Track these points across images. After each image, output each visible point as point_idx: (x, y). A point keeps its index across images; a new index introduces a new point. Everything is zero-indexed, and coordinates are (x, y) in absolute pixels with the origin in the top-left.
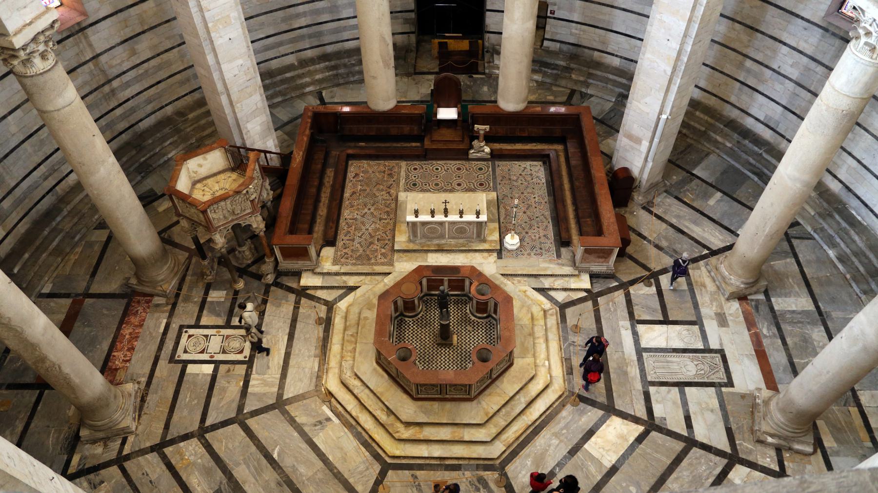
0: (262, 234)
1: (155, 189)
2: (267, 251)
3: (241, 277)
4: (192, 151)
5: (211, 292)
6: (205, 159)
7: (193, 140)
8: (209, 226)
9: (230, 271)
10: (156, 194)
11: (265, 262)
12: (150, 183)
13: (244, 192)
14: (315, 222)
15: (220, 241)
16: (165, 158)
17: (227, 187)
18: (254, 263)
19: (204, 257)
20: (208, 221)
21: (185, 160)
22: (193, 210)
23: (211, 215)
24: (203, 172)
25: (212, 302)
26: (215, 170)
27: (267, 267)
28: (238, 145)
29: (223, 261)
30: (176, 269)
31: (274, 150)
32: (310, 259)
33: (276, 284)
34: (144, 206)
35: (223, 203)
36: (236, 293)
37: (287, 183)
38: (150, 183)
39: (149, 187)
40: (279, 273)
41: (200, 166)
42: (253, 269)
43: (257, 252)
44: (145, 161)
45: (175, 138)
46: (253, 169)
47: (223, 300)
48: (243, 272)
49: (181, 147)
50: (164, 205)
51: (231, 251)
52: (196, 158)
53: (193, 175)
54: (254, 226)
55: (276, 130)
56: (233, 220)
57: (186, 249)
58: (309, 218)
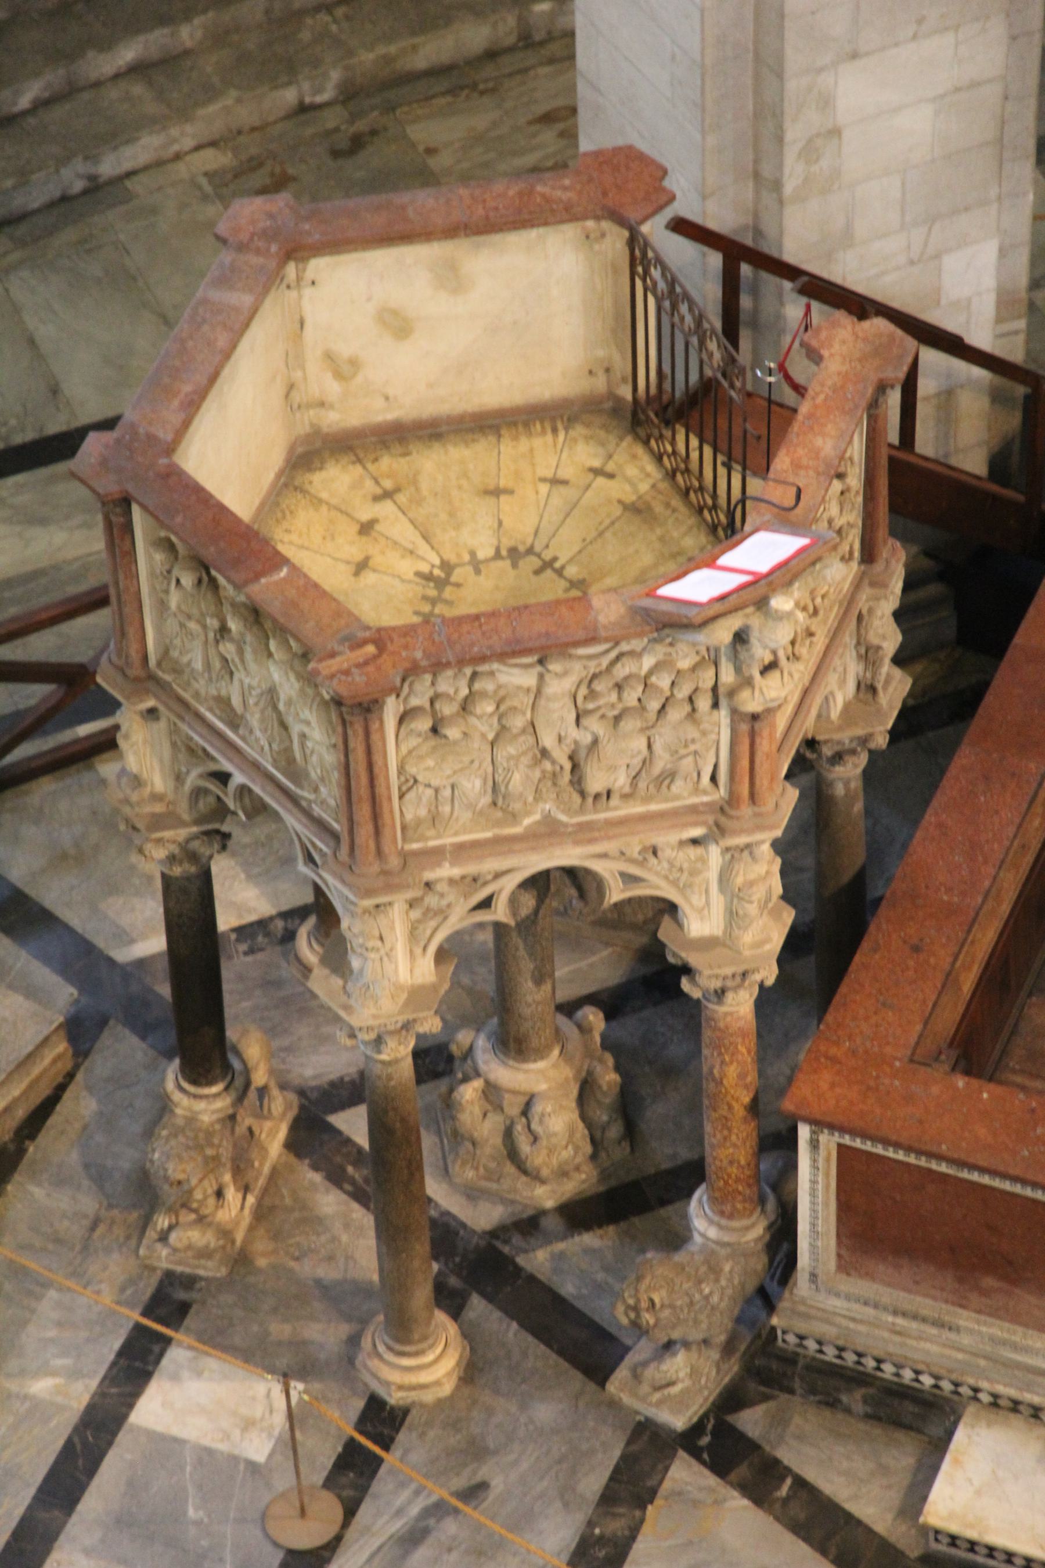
0: (740, 1007)
2: (731, 1146)
3: (449, 1300)
6: (452, 280)
9: (391, 1235)
13: (722, 633)
15: (393, 973)
17: (563, 550)
18: (579, 1215)
20: (363, 786)
21: (297, 251)
23: (396, 745)
24: (406, 380)
25: (165, 1447)
26: (498, 388)
29: (371, 1138)
31: (981, 338)
33: (722, 1445)
35: (516, 677)
36: (382, 1419)
40: (766, 1364)
41: (398, 325)
42: (560, 1262)
43: (631, 1131)
45: (188, 34)
47: (258, 1449)
48: (479, 1271)
49: (214, 116)
52: (381, 258)
53: (321, 383)
54: (701, 921)
56: (549, 832)
57: (83, 960)
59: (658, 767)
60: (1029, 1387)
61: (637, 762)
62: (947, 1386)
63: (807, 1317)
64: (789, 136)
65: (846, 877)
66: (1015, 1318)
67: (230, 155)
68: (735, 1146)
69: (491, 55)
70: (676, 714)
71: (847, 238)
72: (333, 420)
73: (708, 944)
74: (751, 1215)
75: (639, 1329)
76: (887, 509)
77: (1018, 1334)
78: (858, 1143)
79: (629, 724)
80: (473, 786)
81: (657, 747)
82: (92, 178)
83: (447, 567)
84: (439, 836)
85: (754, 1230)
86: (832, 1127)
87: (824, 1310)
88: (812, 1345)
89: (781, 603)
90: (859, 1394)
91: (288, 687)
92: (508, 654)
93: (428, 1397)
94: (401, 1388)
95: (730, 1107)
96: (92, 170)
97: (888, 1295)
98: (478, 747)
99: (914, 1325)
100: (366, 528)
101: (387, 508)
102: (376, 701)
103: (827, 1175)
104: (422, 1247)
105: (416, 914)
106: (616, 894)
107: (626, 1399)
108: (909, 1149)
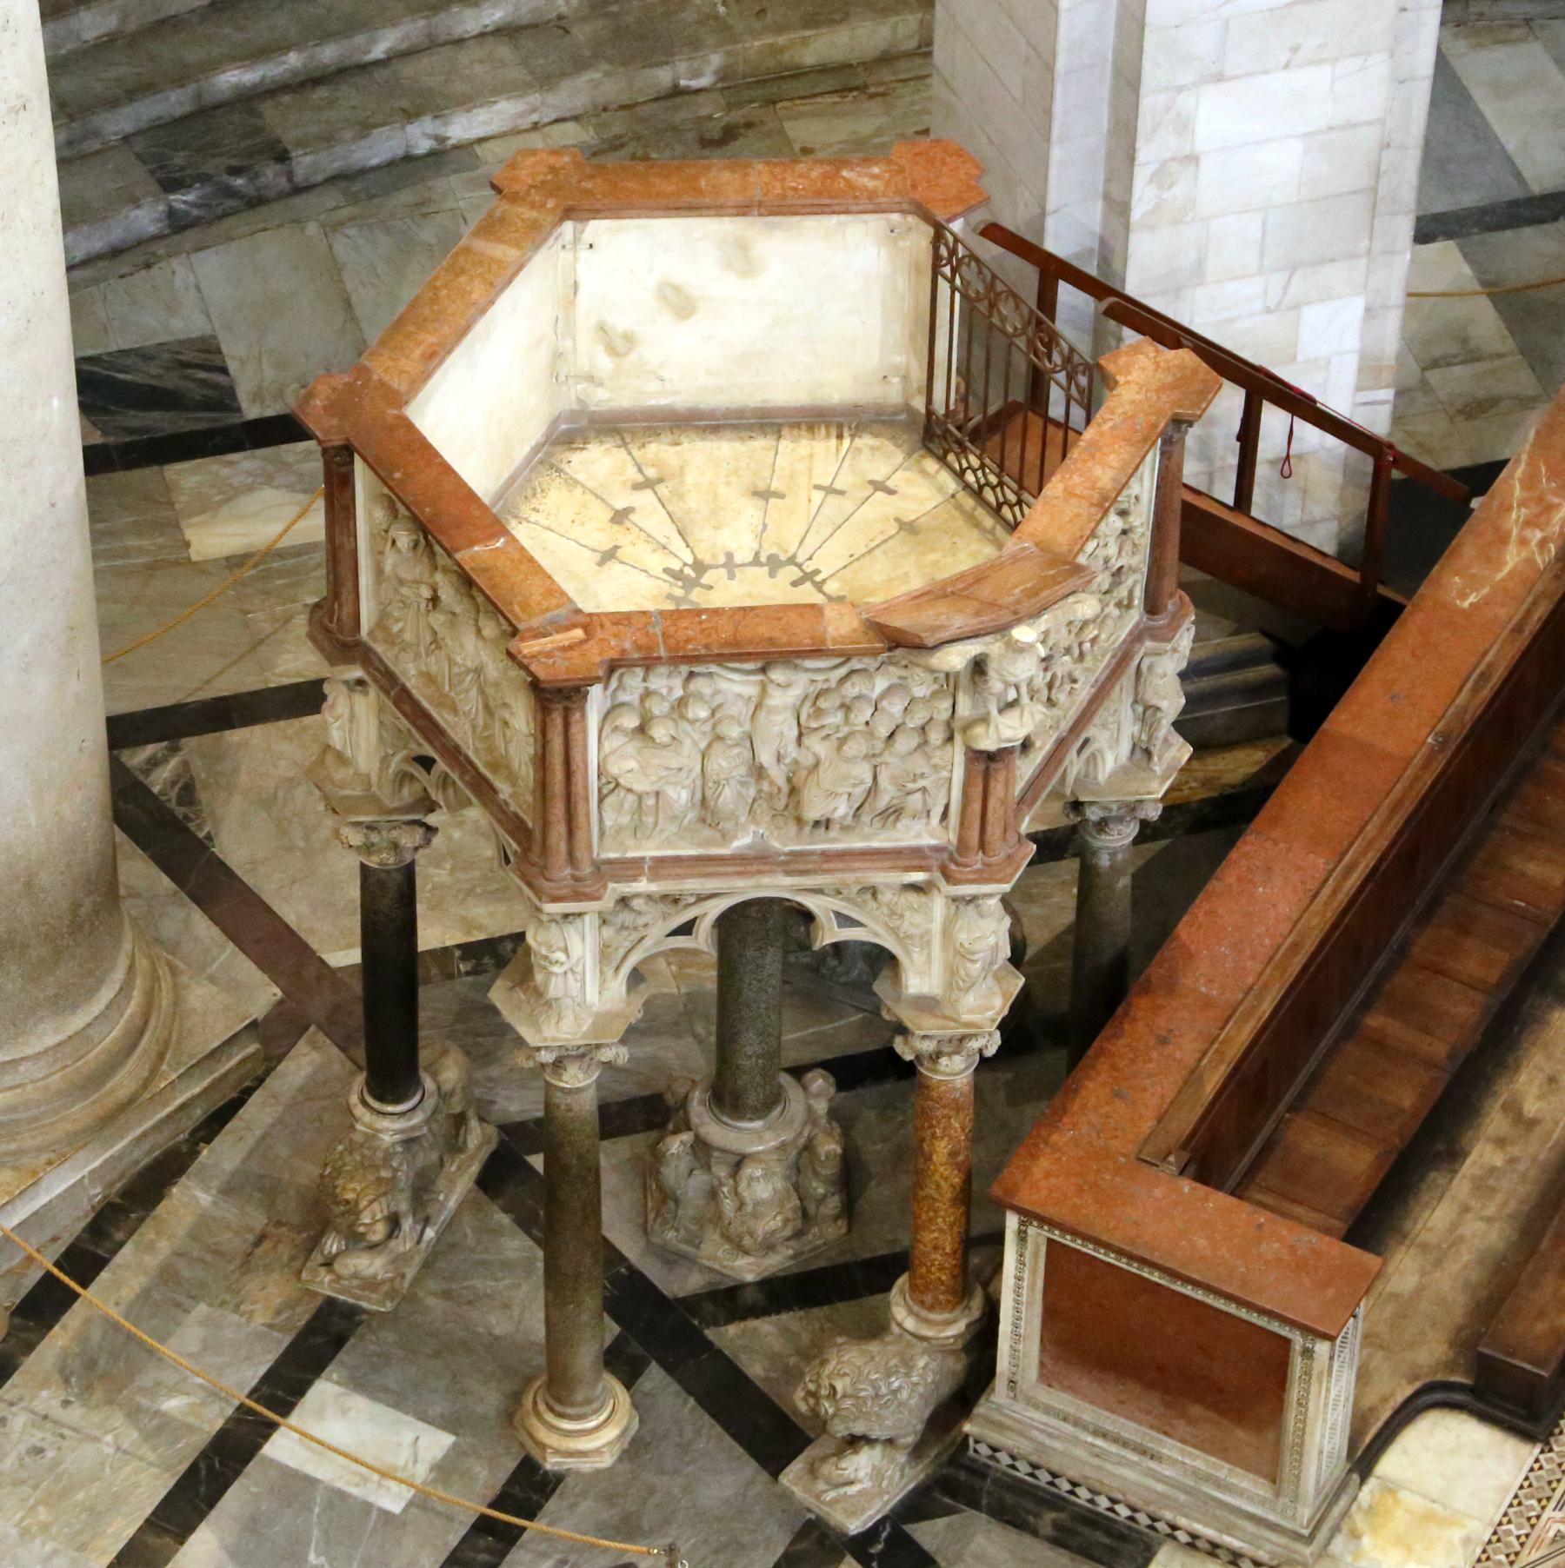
0: (954, 1074)
1: (234, 351)
3: (623, 1364)
4: (664, 152)
5: (324, 1390)
6: (743, 262)
7: (701, 71)
8: (539, 836)
9: (557, 1283)
10: (225, 399)
11: (876, 1328)
12: (231, 298)
13: (956, 658)
14: (1454, 1156)
15: (584, 994)
16: (419, 136)
17: (826, 563)
18: (781, 1293)
19: (392, 1074)
22: (473, 649)
23: (601, 743)
24: (682, 366)
25: (297, 1486)
27: (879, 1379)
28: (1058, 243)
30: (124, 1082)
31: (1338, 402)
32: (1272, 1467)
34: (96, 461)
35: (735, 685)
37: (1344, 720)
38: (231, 298)
39: (187, 324)
42: (755, 1344)
43: (849, 1210)
44: (248, 99)
46: (1106, 497)
47: (393, 1500)
49: (576, 92)
50: (252, 514)
51: (640, 1112)
53: (589, 354)
55: (1427, 231)
56: (756, 860)
58: (1407, 1096)
59: (883, 802)
60: (1229, 1529)
61: (859, 792)
62: (1143, 1519)
63: (1000, 1426)
64: (1141, 156)
65: (1107, 955)
66: (1222, 1451)
67: (592, 132)
68: (940, 1230)
69: (886, 59)
70: (905, 743)
71: (1198, 273)
72: (603, 399)
73: (927, 1004)
74: (954, 1308)
75: (822, 1424)
76: (1176, 557)
77: (1223, 1470)
78: (1067, 1240)
79: (856, 747)
80: (680, 796)
81: (884, 781)
82: (441, 140)
83: (700, 567)
84: (637, 848)
85: (954, 1327)
86: (1043, 1220)
87: (1020, 1422)
88: (1004, 1459)
89: (1024, 633)
90: (1050, 1516)
91: (494, 667)
92: (732, 654)
93: (586, 1466)
94: (557, 1452)
95: (938, 1186)
96: (441, 131)
97: (1089, 1413)
98: (687, 756)
99: (1113, 1448)
100: (620, 516)
101: (645, 498)
102: (577, 690)
103: (1034, 1272)
104: (591, 1301)
105: (608, 932)
106: (829, 934)
107: (797, 1491)
108: (1120, 1252)
